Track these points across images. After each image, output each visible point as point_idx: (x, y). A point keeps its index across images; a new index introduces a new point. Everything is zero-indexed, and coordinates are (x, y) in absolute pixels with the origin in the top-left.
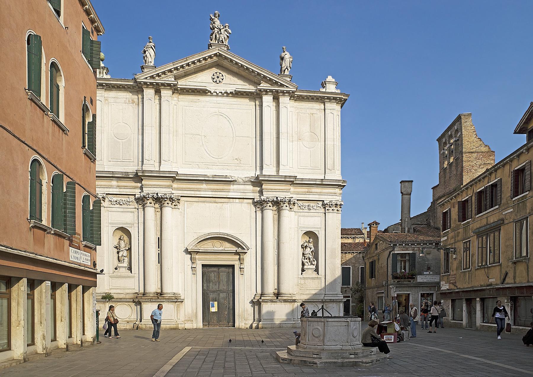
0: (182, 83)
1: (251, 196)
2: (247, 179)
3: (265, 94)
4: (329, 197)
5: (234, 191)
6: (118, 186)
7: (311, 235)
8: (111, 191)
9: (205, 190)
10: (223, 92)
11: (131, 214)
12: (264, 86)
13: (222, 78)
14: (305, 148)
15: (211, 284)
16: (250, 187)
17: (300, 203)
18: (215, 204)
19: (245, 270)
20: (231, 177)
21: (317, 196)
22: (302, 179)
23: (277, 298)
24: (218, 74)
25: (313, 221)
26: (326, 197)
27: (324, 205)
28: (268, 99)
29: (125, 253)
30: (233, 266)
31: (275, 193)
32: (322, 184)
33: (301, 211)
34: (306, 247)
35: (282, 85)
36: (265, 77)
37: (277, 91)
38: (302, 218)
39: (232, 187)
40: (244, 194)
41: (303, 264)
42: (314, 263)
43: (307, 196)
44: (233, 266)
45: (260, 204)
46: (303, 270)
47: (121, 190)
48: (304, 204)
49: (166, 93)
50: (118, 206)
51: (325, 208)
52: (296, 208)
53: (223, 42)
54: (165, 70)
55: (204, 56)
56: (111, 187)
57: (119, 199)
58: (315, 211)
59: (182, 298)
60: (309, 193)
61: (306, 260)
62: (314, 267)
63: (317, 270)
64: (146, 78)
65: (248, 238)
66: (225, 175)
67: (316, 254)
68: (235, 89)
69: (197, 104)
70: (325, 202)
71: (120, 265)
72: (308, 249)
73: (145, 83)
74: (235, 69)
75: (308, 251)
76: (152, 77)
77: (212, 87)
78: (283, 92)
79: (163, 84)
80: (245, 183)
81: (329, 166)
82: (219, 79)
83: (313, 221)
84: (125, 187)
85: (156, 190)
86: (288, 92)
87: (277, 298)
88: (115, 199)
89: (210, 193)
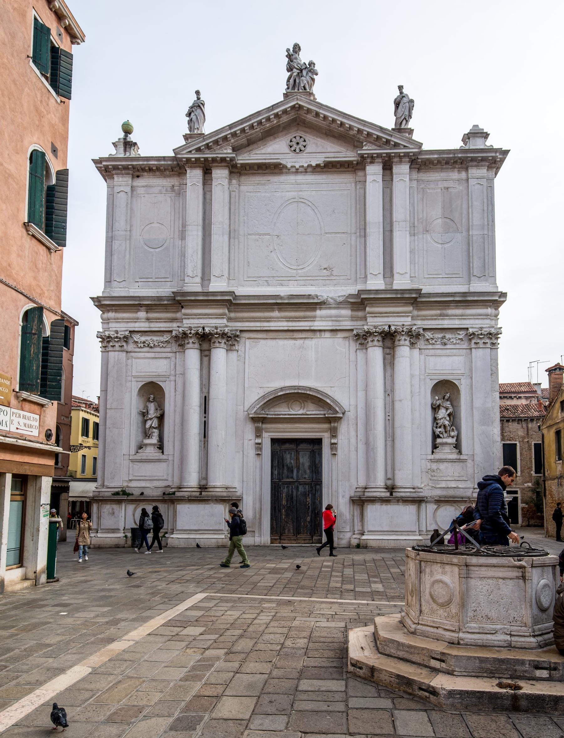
0: (244, 158)
1: (348, 324)
2: (341, 299)
3: (372, 163)
4: (477, 322)
5: (322, 319)
6: (148, 319)
8: (138, 326)
10: (306, 165)
11: (165, 362)
12: (368, 149)
13: (304, 144)
14: (436, 244)
16: (347, 312)
17: (428, 335)
18: (292, 342)
19: (339, 446)
20: (317, 296)
21: (457, 322)
23: (391, 494)
24: (298, 138)
26: (472, 322)
28: (374, 172)
29: (155, 423)
30: (318, 442)
31: (386, 319)
33: (430, 347)
34: (439, 406)
35: (396, 145)
37: (388, 155)
38: (432, 359)
39: (319, 313)
40: (337, 324)
41: (435, 436)
43: (440, 322)
44: (318, 442)
46: (435, 447)
47: (152, 325)
49: (220, 175)
52: (421, 343)
53: (305, 89)
54: (217, 137)
56: (136, 320)
57: (148, 338)
59: (238, 494)
61: (439, 430)
62: (453, 441)
64: (190, 152)
65: (342, 395)
66: (307, 294)
68: (323, 159)
69: (267, 187)
70: (471, 330)
71: (147, 441)
73: (188, 160)
75: (442, 413)
76: (198, 150)
77: (289, 160)
78: (399, 156)
79: (214, 160)
80: (340, 305)
82: (300, 146)
84: (158, 320)
85: (203, 322)
86: (407, 155)
87: (391, 494)
88: (143, 339)
89: (285, 324)
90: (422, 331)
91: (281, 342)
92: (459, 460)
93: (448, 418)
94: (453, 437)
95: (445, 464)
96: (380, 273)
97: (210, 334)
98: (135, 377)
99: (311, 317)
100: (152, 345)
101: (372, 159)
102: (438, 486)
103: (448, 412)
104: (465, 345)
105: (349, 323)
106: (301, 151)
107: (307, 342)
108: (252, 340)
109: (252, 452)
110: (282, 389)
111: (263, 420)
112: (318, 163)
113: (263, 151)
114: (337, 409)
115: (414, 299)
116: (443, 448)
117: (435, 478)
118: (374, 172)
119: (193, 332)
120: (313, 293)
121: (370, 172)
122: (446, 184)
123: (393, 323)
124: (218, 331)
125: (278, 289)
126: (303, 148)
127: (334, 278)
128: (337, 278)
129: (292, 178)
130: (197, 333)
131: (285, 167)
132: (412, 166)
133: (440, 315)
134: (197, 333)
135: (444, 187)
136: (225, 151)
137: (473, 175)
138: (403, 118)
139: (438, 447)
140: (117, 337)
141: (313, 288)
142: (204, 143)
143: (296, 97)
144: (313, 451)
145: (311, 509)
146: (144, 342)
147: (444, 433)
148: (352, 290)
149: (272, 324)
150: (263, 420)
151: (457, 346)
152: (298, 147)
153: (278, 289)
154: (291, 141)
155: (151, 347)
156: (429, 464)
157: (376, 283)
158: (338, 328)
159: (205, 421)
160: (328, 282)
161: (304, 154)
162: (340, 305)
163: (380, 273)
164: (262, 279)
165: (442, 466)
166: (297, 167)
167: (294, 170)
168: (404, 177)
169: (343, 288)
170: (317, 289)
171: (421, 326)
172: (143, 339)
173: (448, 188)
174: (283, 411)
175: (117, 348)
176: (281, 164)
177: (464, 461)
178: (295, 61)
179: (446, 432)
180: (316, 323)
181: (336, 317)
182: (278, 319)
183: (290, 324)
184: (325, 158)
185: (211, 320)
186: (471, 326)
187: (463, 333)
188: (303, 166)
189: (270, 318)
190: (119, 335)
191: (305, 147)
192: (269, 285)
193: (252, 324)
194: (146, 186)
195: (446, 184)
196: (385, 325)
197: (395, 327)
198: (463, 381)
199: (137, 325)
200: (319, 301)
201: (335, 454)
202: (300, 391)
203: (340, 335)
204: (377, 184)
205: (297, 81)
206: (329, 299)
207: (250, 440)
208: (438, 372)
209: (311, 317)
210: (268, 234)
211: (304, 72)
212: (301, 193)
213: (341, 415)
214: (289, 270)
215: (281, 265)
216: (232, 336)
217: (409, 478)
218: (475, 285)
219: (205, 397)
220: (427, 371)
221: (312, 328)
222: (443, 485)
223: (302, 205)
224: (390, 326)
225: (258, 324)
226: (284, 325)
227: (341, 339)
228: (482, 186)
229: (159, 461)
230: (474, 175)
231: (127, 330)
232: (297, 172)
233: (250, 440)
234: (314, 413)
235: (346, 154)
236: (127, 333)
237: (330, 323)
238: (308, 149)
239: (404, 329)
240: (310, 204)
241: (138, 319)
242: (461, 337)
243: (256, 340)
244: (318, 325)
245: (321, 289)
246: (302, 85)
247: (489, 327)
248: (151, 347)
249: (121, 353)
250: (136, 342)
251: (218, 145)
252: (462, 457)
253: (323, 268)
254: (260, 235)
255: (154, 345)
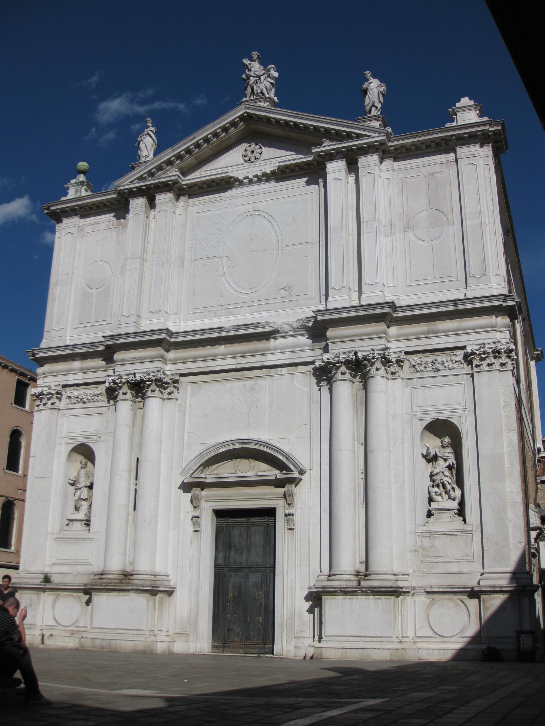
1: (308, 356)
2: (298, 325)
4: (478, 336)
5: (277, 352)
7: (443, 428)
9: (224, 357)
11: (97, 418)
12: (328, 146)
15: (232, 553)
17: (414, 359)
18: (241, 383)
20: (267, 323)
21: (451, 339)
22: (411, 307)
25: (446, 396)
26: (471, 337)
27: (468, 359)
28: (336, 169)
30: (271, 512)
32: (458, 312)
33: (418, 375)
36: (327, 130)
37: (350, 149)
38: (420, 391)
39: (273, 343)
42: (453, 494)
43: (429, 341)
44: (271, 512)
45: (324, 374)
47: (87, 376)
48: (424, 360)
50: (80, 405)
51: (470, 363)
54: (160, 162)
55: (221, 125)
56: (70, 372)
57: (81, 392)
58: (449, 373)
60: (432, 333)
62: (455, 505)
63: (461, 512)
64: (133, 181)
65: (302, 449)
66: (254, 321)
67: (457, 470)
68: (278, 165)
69: (218, 204)
70: (469, 349)
72: (441, 462)
73: (130, 191)
74: (280, 132)
77: (240, 173)
80: (296, 331)
81: (473, 270)
83: (446, 396)
84: (93, 370)
88: (76, 393)
89: (232, 361)
90: (403, 356)
91: (228, 385)
92: (463, 533)
93: (447, 473)
94: (454, 499)
95: (443, 539)
96: (344, 287)
97: (142, 381)
98: (65, 438)
99: (263, 350)
100: (85, 400)
101: (331, 156)
102: (433, 572)
103: (447, 464)
104: (466, 369)
105: (311, 353)
106: (256, 159)
107: (261, 382)
108: (194, 385)
109: (189, 527)
110: (223, 444)
111: (203, 486)
112: (272, 169)
113: (215, 166)
114: (292, 467)
115: (386, 315)
116: (440, 515)
117: (428, 560)
118: (336, 169)
119: (124, 380)
120: (262, 321)
121: (330, 170)
122: (430, 170)
123: (360, 349)
124: (151, 377)
125: (226, 319)
126: (258, 156)
127: (294, 298)
128: (298, 298)
129: (246, 190)
130: (128, 382)
131: (237, 180)
132: (384, 156)
133: (428, 333)
134: (128, 382)
135: (428, 174)
136: (171, 174)
137: (462, 154)
138: (371, 104)
139: (433, 515)
140: (49, 394)
141: (268, 314)
142: (147, 170)
143: (243, 106)
144: (268, 525)
145: (263, 606)
146: (77, 398)
147: (443, 494)
148: (305, 311)
149: (218, 363)
150: (203, 486)
151: (455, 372)
152: (252, 156)
153: (226, 319)
154: (246, 151)
155: (84, 403)
156: (418, 540)
157: (342, 299)
158: (297, 361)
159: (136, 490)
160: (286, 304)
161: (259, 162)
162: (296, 331)
163: (344, 287)
164: (209, 309)
165: (439, 542)
166: (251, 177)
167: (247, 181)
168: (371, 170)
169: (304, 310)
170: (272, 314)
171: (401, 349)
172: (76, 393)
173: (433, 174)
174: (227, 470)
175: (49, 406)
176: (231, 177)
177: (470, 533)
178: (252, 69)
179: (446, 493)
180: (270, 357)
181: (295, 346)
182: (224, 356)
183: (239, 361)
184: (279, 162)
185: (144, 364)
186: (471, 343)
187: (461, 353)
188: (247, 178)
189: (215, 356)
190: (51, 391)
191: (260, 154)
192: (216, 316)
193: (194, 365)
194: (93, 224)
195: (430, 170)
196: (351, 352)
197: (363, 353)
198: (463, 420)
199: (71, 377)
200: (271, 329)
201: (291, 529)
202: (246, 446)
203: (301, 369)
204: (339, 182)
205: (255, 88)
206: (284, 326)
207: (188, 512)
208: (429, 408)
209: (263, 350)
210: (218, 256)
211: (262, 78)
212: (256, 205)
213: (296, 475)
214: (240, 295)
215: (231, 290)
216: (170, 381)
217: (393, 559)
218: (474, 288)
219: (138, 459)
220: (415, 408)
221: (266, 364)
222: (440, 569)
223: (258, 218)
224: (356, 353)
225: (201, 364)
226: (231, 363)
227: (302, 375)
228: (475, 166)
229: (85, 540)
230: (464, 154)
231: (59, 385)
232: (251, 182)
233: (188, 512)
234: (266, 473)
235: (290, 157)
236: (59, 388)
237: (287, 356)
238: (263, 157)
239: (375, 355)
240: (266, 215)
241: (72, 370)
242: (457, 359)
243: (199, 384)
244: (272, 359)
245: (277, 313)
246: (259, 91)
247: (494, 343)
248: (84, 403)
249: (52, 411)
250: (70, 397)
251: (162, 170)
252: (467, 527)
253: (280, 288)
254: (208, 258)
255: (88, 399)
